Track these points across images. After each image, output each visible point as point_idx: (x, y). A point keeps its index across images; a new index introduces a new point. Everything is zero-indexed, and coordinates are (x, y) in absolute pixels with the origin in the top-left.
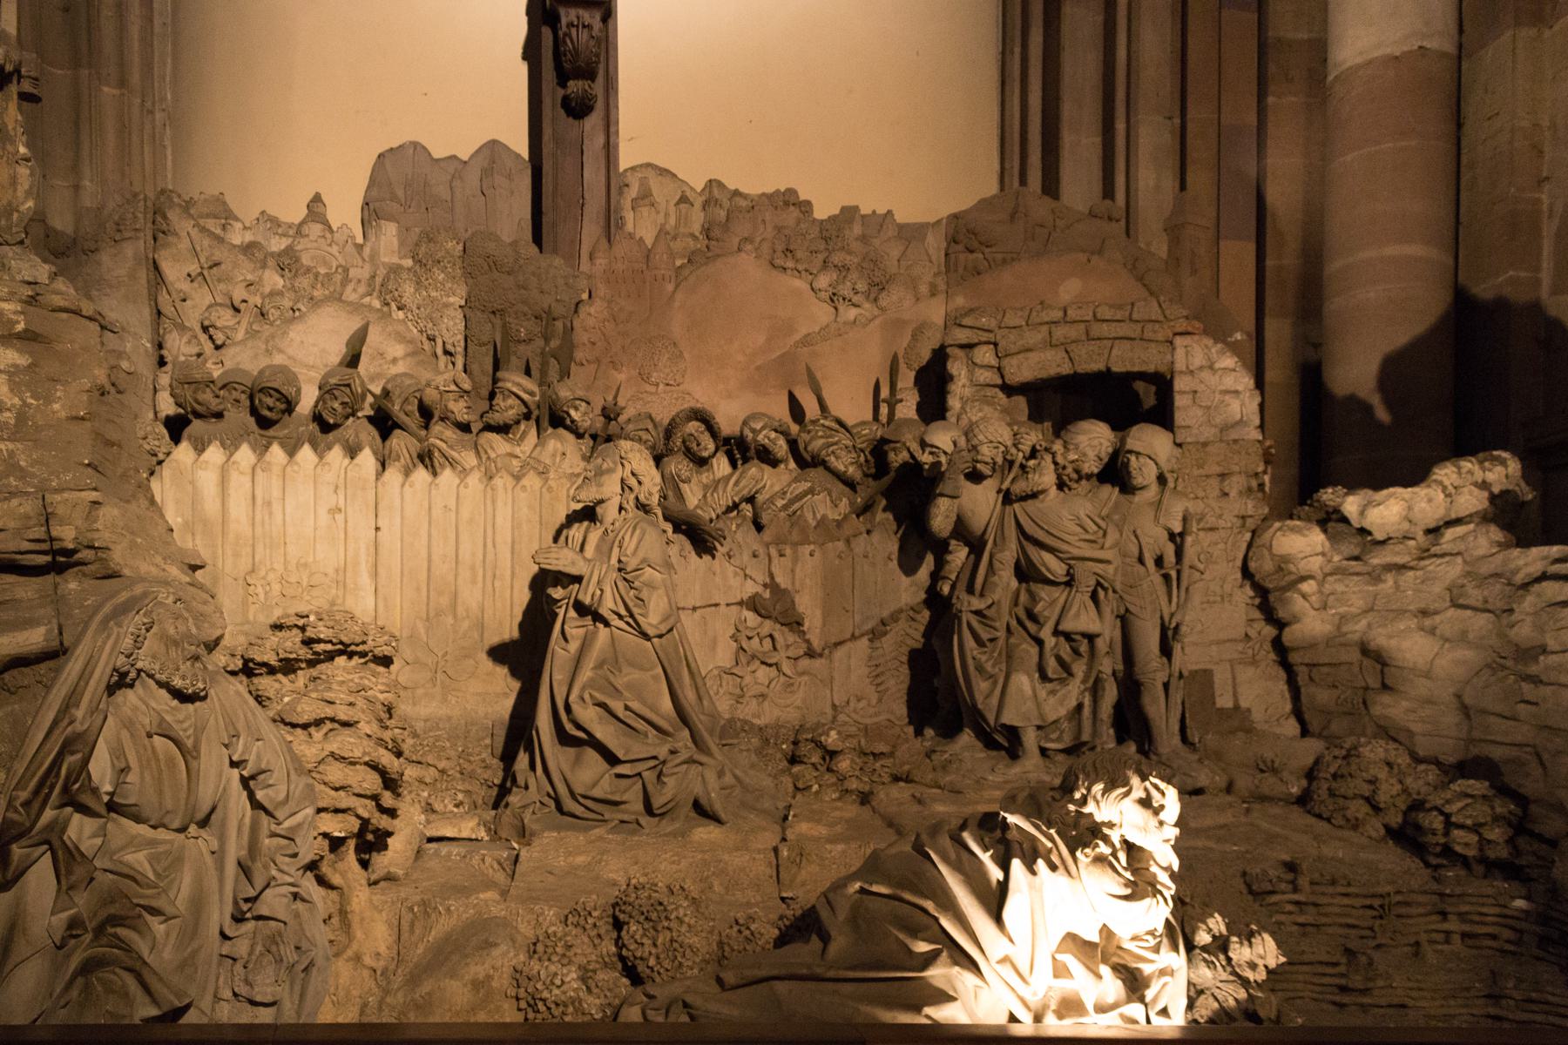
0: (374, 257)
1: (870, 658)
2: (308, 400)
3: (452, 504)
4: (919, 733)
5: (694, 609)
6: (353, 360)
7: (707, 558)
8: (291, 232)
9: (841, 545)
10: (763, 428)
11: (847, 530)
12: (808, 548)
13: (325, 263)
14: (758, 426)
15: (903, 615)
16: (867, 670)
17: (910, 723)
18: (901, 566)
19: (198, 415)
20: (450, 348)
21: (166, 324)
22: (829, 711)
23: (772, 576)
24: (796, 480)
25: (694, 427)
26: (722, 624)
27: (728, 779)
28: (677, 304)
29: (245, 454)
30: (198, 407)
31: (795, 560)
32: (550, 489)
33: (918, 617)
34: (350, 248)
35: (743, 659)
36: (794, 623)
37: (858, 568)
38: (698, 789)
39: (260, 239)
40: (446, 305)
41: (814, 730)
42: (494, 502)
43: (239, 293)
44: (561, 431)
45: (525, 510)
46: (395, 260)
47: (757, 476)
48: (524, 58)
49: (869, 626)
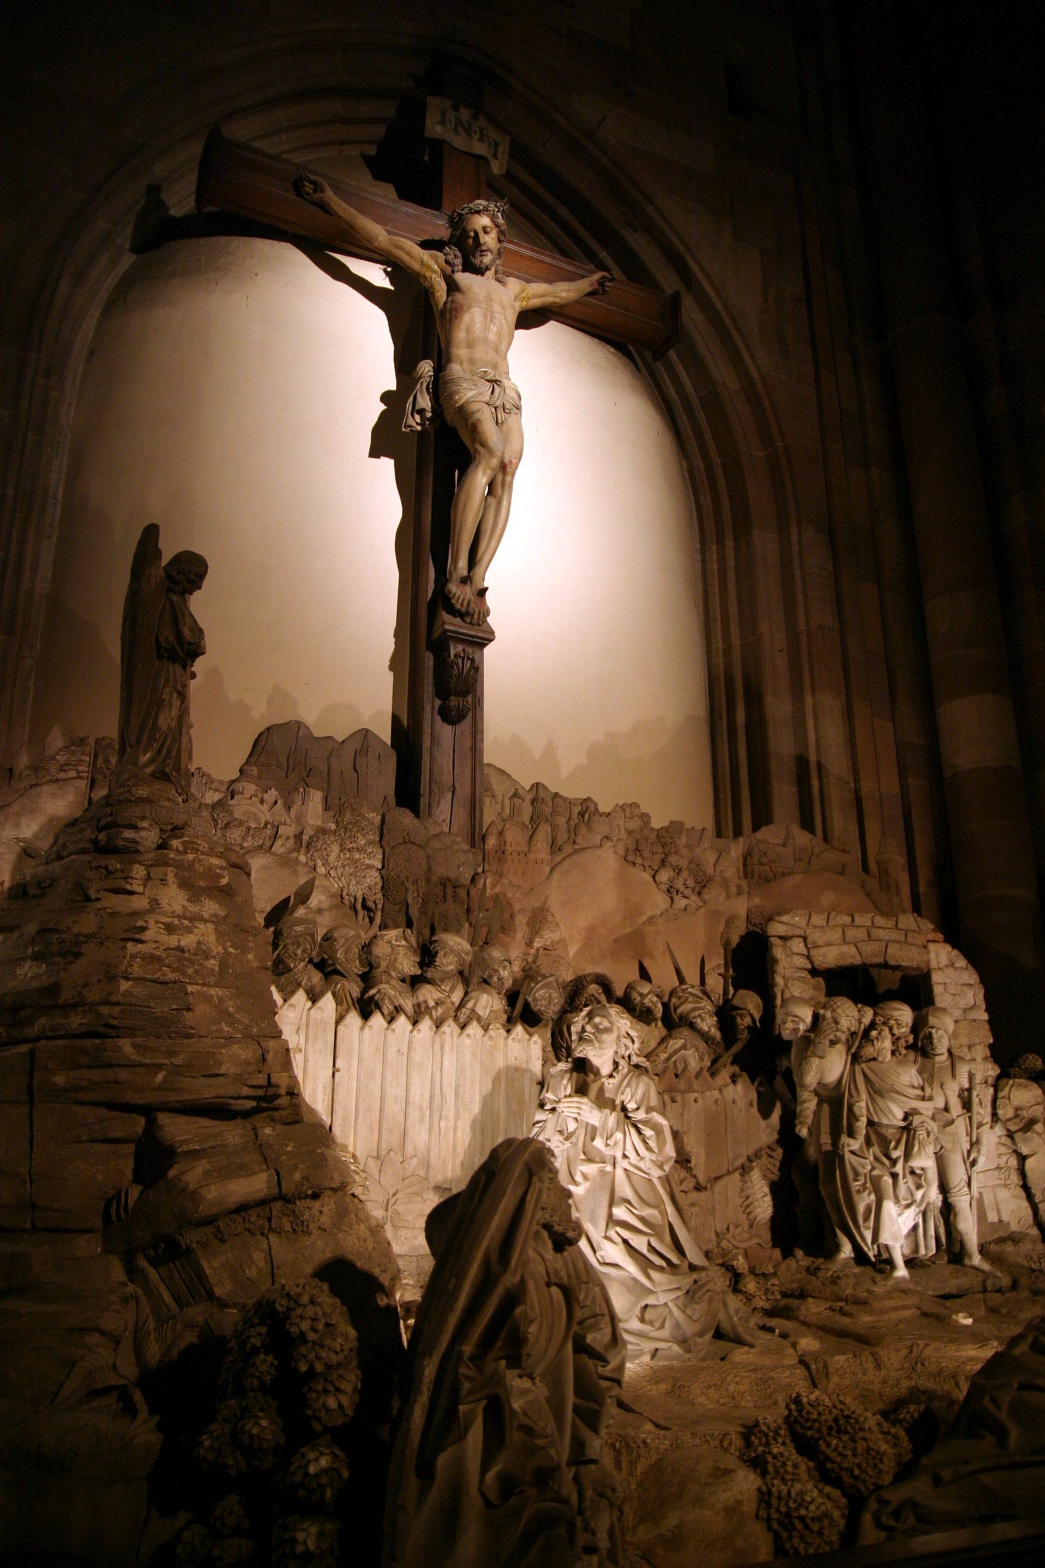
0: (299, 819)
1: (742, 1190)
3: (405, 1049)
4: (787, 1254)
8: (224, 788)
9: (716, 1093)
10: (649, 993)
13: (256, 819)
14: (645, 991)
15: (763, 1153)
16: (741, 1201)
17: (774, 1246)
18: (760, 1110)
20: (370, 904)
22: (713, 1237)
25: (594, 989)
28: (554, 883)
31: (684, 1106)
32: (491, 1038)
33: (774, 1154)
40: (370, 867)
42: (442, 1048)
45: (468, 1057)
49: (738, 1163)
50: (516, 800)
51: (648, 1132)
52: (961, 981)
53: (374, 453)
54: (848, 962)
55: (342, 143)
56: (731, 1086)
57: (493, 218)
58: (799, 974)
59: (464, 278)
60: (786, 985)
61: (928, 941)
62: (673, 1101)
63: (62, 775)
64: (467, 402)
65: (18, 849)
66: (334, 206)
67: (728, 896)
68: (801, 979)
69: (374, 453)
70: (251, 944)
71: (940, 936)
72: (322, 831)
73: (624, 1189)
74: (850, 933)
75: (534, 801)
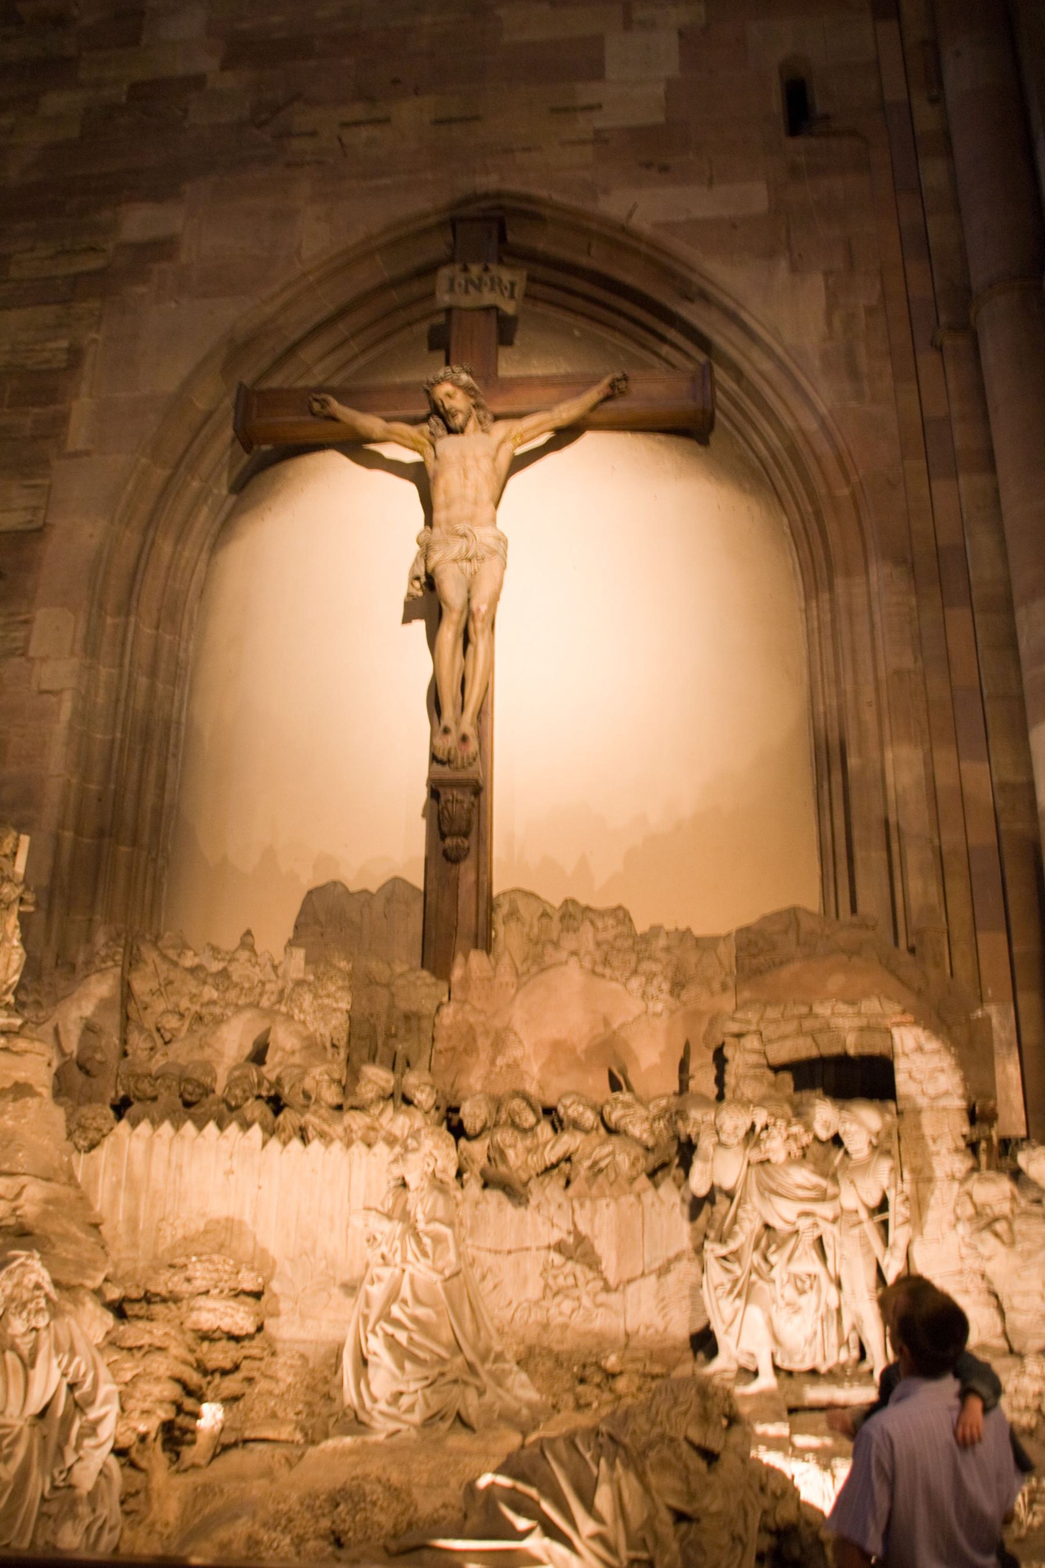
1: (657, 1293)
2: (220, 1087)
5: (509, 1252)
6: (259, 1056)
7: (522, 1209)
9: (632, 1199)
10: (573, 1103)
12: (603, 1202)
19: (139, 1099)
20: (335, 1042)
21: (131, 1027)
23: (575, 1225)
24: (602, 1144)
25: (517, 1104)
26: (532, 1265)
27: (488, 1397)
28: (517, 1003)
29: (166, 1128)
30: (138, 1094)
34: (269, 968)
35: (549, 1294)
36: (592, 1261)
38: (459, 1405)
39: (205, 963)
41: (597, 1355)
43: (184, 1003)
44: (412, 1108)
46: (301, 976)
47: (569, 1141)
48: (423, 816)
49: (656, 1265)
50: (544, 921)
51: (427, 1241)
53: (407, 619)
55: (410, 324)
57: (455, 383)
59: (448, 445)
60: (737, 1085)
62: (582, 1205)
63: (103, 966)
64: (437, 564)
65: (82, 1026)
66: (339, 416)
67: (712, 994)
68: (756, 1078)
69: (407, 619)
70: (10, 1109)
71: (910, 1018)
72: (299, 983)
73: (406, 1292)
74: (808, 1024)
75: (562, 918)
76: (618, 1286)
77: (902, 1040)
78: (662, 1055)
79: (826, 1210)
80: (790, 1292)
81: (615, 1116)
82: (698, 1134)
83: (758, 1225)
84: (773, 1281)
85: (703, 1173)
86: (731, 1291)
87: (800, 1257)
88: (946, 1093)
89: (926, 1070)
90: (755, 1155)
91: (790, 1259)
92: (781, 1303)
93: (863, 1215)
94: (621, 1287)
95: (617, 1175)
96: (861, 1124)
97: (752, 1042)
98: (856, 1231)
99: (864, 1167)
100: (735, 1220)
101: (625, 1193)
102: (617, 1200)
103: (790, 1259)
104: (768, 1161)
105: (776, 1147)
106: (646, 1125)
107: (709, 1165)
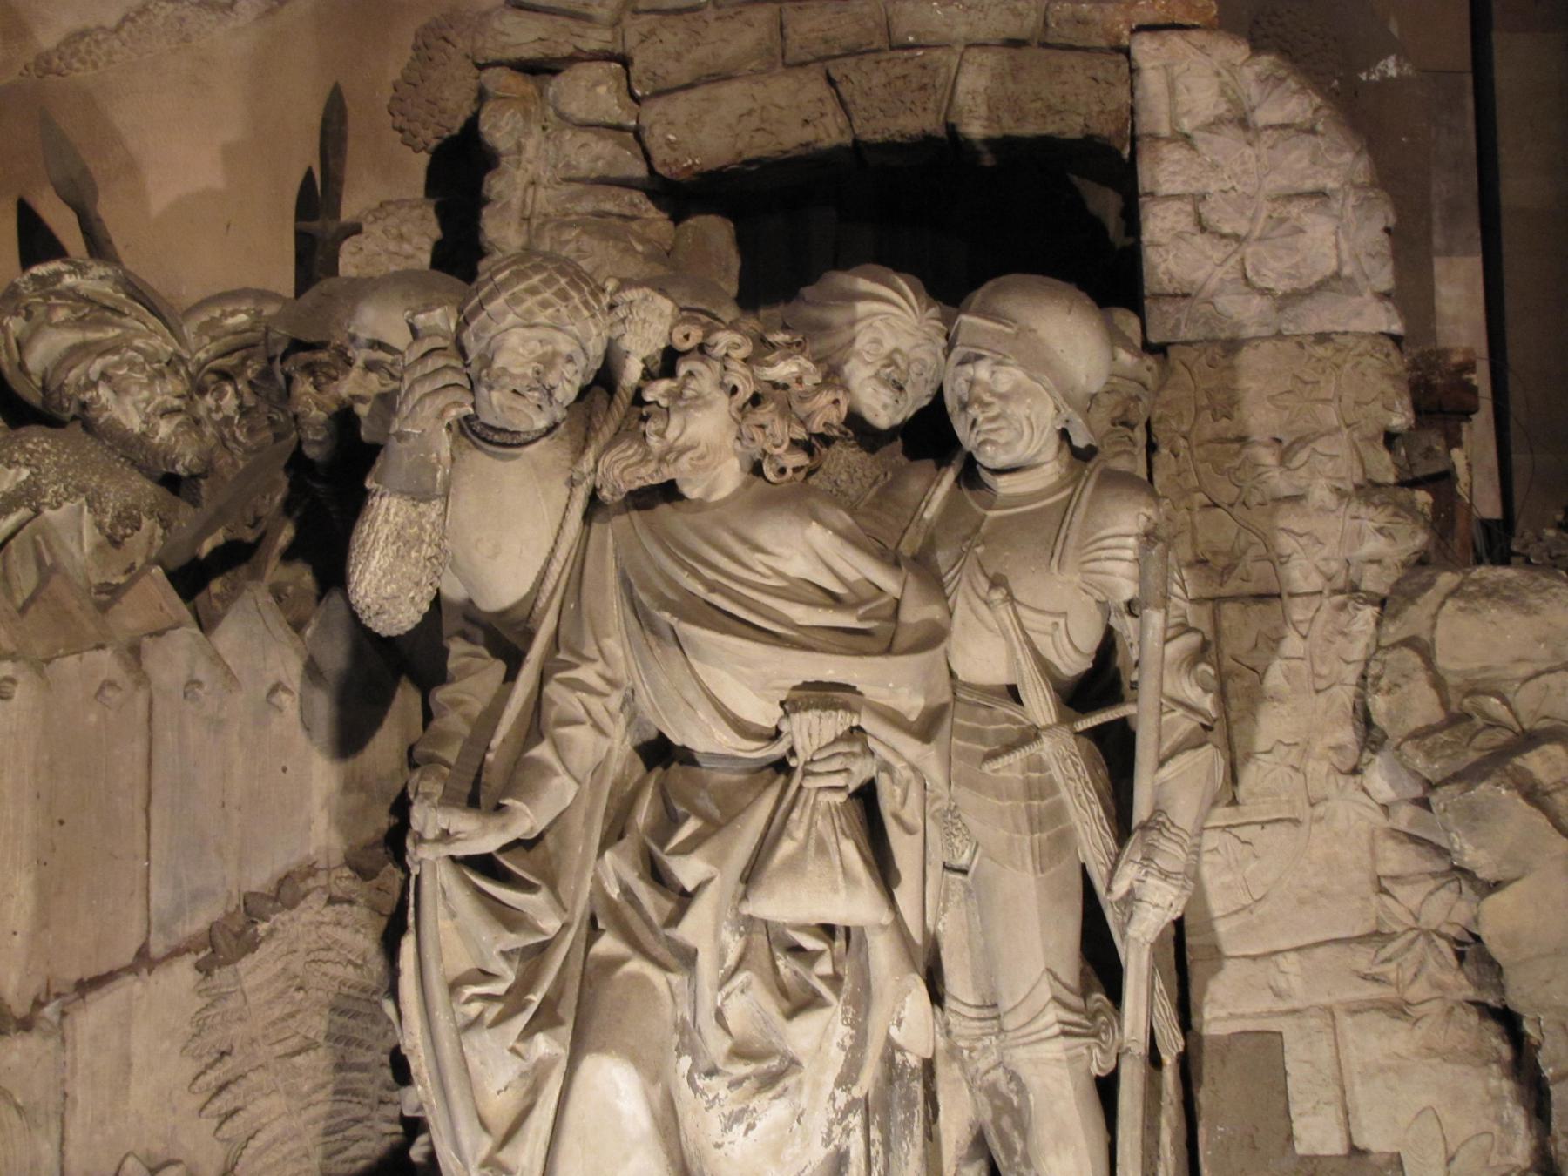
9: (106, 662)
11: (130, 617)
16: (192, 1067)
37: (167, 737)
49: (199, 921)
52: (1277, 182)
54: (791, 137)
56: (188, 634)
58: (586, 206)
61: (1141, 28)
76: (38, 1004)
77: (1172, 90)
78: (230, 154)
79: (895, 684)
80: (749, 1004)
81: (40, 356)
82: (387, 403)
83: (620, 745)
84: (687, 958)
85: (405, 541)
86: (513, 1001)
87: (794, 866)
88: (1333, 283)
89: (1259, 199)
90: (622, 470)
91: (751, 876)
92: (716, 1045)
93: (1040, 706)
94: (50, 1011)
95: (46, 572)
96: (1039, 362)
97: (592, 93)
98: (1010, 767)
99: (1049, 529)
100: (535, 724)
101: (76, 648)
102: (40, 666)
103: (751, 876)
104: (669, 492)
105: (705, 438)
106: (169, 391)
107: (433, 510)
